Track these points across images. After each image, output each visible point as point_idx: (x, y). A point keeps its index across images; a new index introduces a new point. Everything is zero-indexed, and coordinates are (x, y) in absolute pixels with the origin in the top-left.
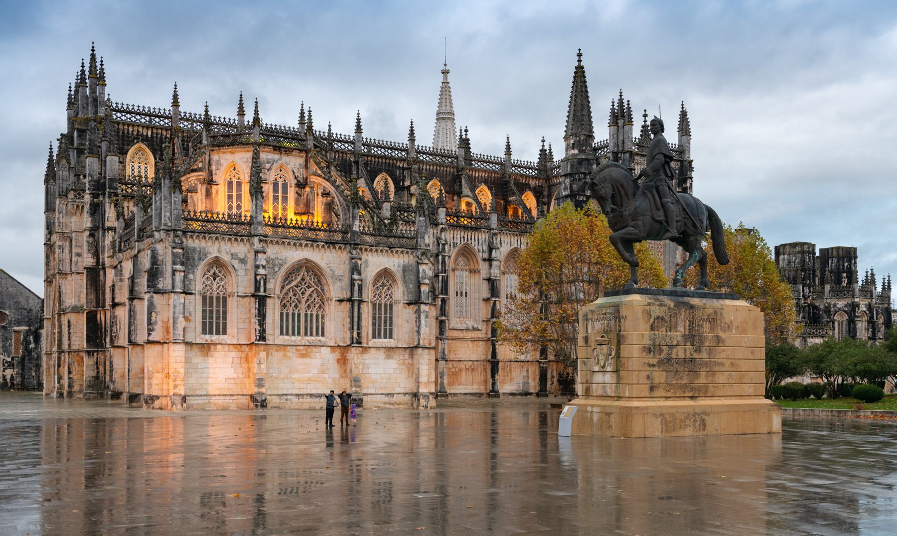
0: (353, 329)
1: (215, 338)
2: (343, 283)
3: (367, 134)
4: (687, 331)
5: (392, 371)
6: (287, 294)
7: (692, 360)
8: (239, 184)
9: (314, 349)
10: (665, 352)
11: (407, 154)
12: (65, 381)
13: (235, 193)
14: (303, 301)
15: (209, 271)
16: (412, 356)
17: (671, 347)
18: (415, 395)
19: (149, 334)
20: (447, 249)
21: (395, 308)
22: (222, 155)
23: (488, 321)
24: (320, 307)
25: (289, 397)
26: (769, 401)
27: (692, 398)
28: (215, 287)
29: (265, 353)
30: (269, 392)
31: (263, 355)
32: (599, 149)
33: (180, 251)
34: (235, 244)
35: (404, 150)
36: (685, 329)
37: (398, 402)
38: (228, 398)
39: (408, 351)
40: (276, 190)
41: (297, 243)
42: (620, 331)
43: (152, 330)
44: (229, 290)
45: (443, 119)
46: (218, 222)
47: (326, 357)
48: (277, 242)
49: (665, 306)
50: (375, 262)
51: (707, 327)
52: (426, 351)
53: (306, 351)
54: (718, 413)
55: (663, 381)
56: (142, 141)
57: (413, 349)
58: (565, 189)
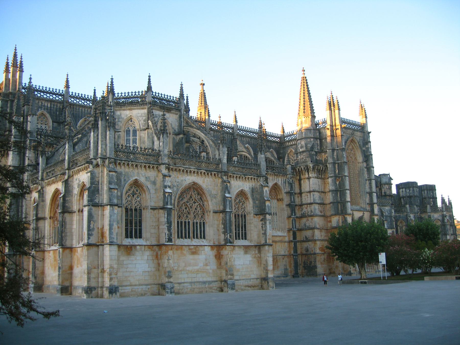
5: (248, 263)
6: (181, 207)
8: (135, 132)
9: (201, 248)
13: (131, 138)
15: (129, 190)
16: (260, 252)
21: (247, 218)
25: (185, 284)
28: (134, 202)
29: (172, 251)
31: (170, 252)
33: (114, 173)
37: (253, 285)
38: (144, 287)
39: (257, 248)
47: (207, 254)
48: (176, 170)
50: (238, 185)
53: (195, 251)
57: (259, 247)
58: (301, 148)
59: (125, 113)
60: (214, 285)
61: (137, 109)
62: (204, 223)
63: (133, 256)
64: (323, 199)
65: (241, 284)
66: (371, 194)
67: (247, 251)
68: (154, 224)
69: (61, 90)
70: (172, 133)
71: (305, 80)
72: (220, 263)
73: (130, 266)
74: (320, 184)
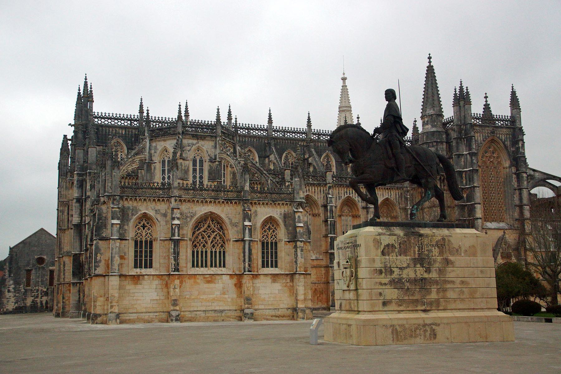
0: (244, 261)
1: (144, 271)
2: (239, 228)
3: (276, 124)
5: (277, 292)
6: (197, 237)
9: (218, 277)
10: (395, 273)
11: (306, 136)
12: (61, 305)
13: (166, 168)
14: (209, 242)
15: (140, 223)
16: (292, 280)
17: (401, 269)
18: (295, 310)
19: (95, 269)
21: (279, 245)
22: (158, 143)
23: (327, 252)
24: (222, 246)
25: (198, 313)
26: (501, 314)
27: (424, 311)
28: (144, 234)
30: (183, 310)
31: (177, 282)
32: (448, 123)
33: (117, 210)
34: (158, 203)
35: (304, 133)
37: (282, 315)
39: (289, 277)
40: (194, 164)
41: (204, 202)
42: (357, 257)
43: (98, 266)
44: (154, 236)
45: (343, 111)
46: (156, 189)
48: (189, 201)
49: (395, 235)
52: (302, 276)
54: (447, 324)
55: (395, 297)
56: (119, 137)
57: (292, 276)
59: (160, 145)
60: (233, 314)
61: (170, 139)
62: (224, 252)
63: (140, 286)
65: (267, 314)
66: (521, 207)
68: (164, 255)
69: (136, 115)
70: (207, 161)
71: (430, 70)
72: (241, 292)
73: (136, 294)
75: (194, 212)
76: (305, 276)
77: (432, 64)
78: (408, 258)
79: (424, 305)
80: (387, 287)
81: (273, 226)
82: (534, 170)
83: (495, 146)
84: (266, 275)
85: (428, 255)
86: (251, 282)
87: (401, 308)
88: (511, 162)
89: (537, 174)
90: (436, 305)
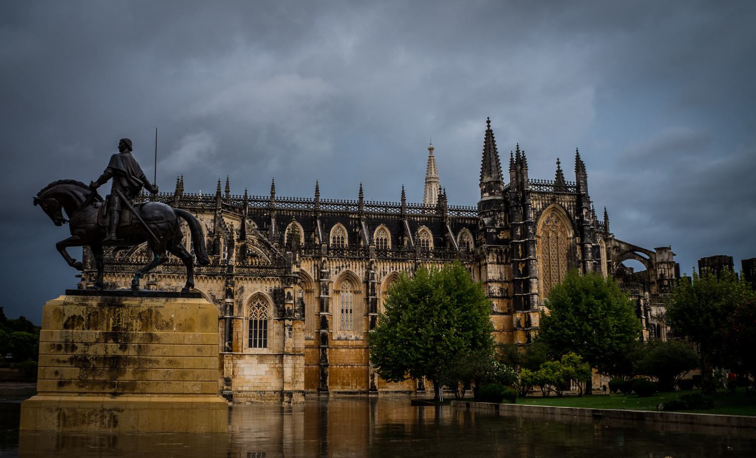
3: (322, 198)
4: (110, 330)
5: (264, 374)
7: (119, 357)
11: (359, 208)
17: (86, 344)
20: (376, 278)
21: (268, 324)
35: (356, 205)
36: (108, 326)
39: (278, 357)
48: (169, 277)
51: (137, 324)
52: (290, 357)
54: (135, 409)
55: (77, 375)
64: (507, 291)
67: (262, 361)
74: (502, 270)
75: (174, 288)
76: (293, 356)
77: (491, 128)
78: (99, 331)
79: (114, 387)
80: (65, 365)
81: (263, 303)
82: (620, 242)
83: (558, 215)
84: (252, 355)
85: (126, 329)
86: (231, 362)
87: (83, 390)
88: (575, 232)
89: (623, 246)
90: (131, 388)
